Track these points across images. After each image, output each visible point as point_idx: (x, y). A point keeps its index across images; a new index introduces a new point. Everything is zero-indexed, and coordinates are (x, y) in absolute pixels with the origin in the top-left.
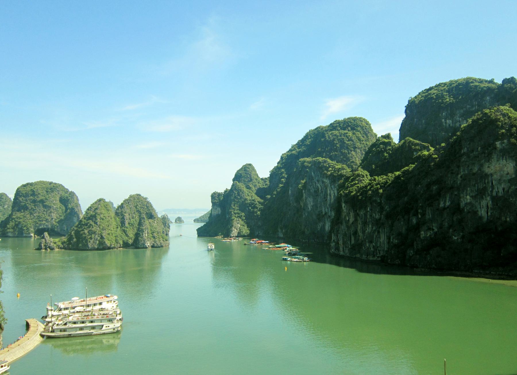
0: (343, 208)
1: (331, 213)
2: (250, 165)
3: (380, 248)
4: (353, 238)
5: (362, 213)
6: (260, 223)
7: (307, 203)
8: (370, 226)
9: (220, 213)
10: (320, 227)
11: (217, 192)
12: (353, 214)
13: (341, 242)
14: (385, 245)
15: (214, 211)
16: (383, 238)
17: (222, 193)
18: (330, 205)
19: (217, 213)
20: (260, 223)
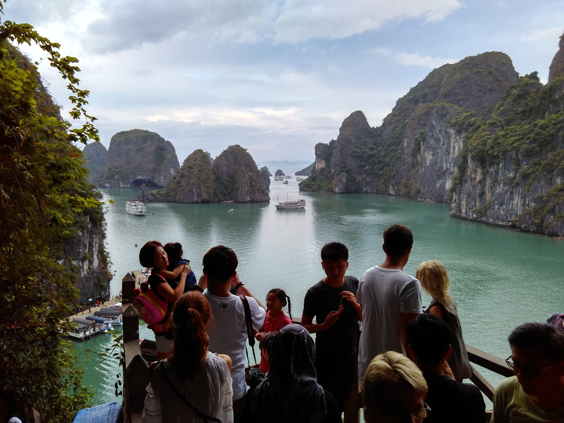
0: (469, 164)
1: (453, 169)
3: (512, 211)
4: (478, 199)
5: (492, 170)
7: (425, 156)
8: (502, 185)
9: (324, 166)
13: (464, 202)
14: (519, 208)
15: (318, 165)
16: (517, 200)
17: (327, 144)
18: (452, 159)
19: (322, 167)
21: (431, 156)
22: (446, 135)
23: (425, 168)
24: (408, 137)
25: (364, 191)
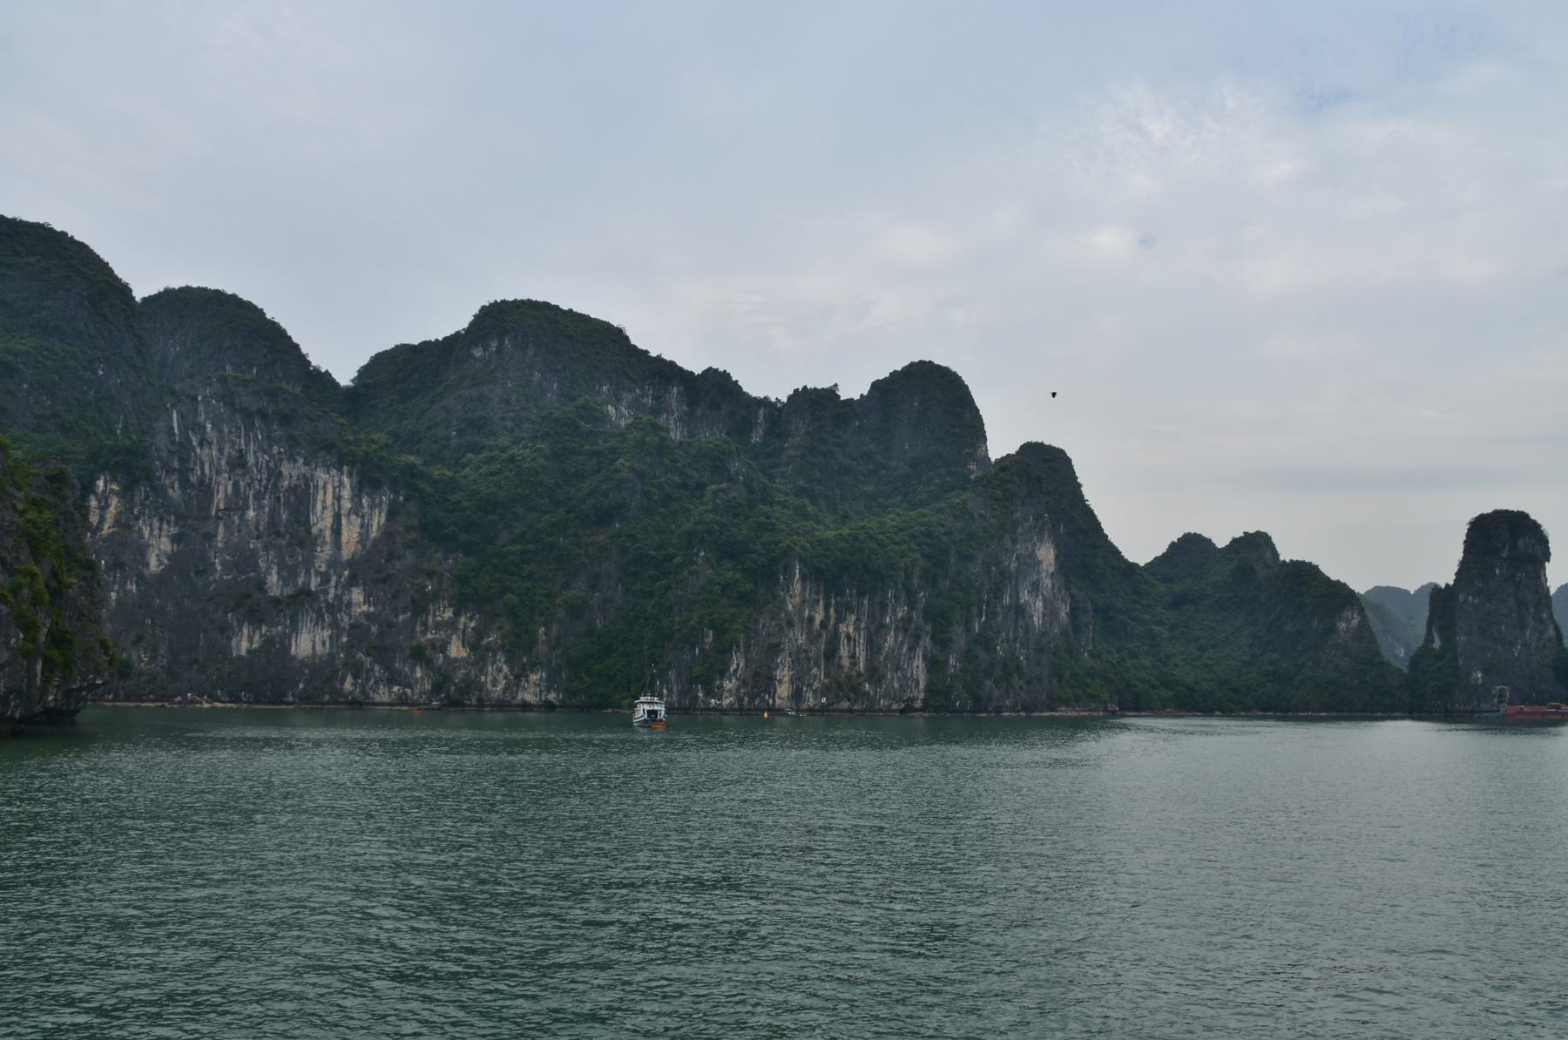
23: (141, 580)
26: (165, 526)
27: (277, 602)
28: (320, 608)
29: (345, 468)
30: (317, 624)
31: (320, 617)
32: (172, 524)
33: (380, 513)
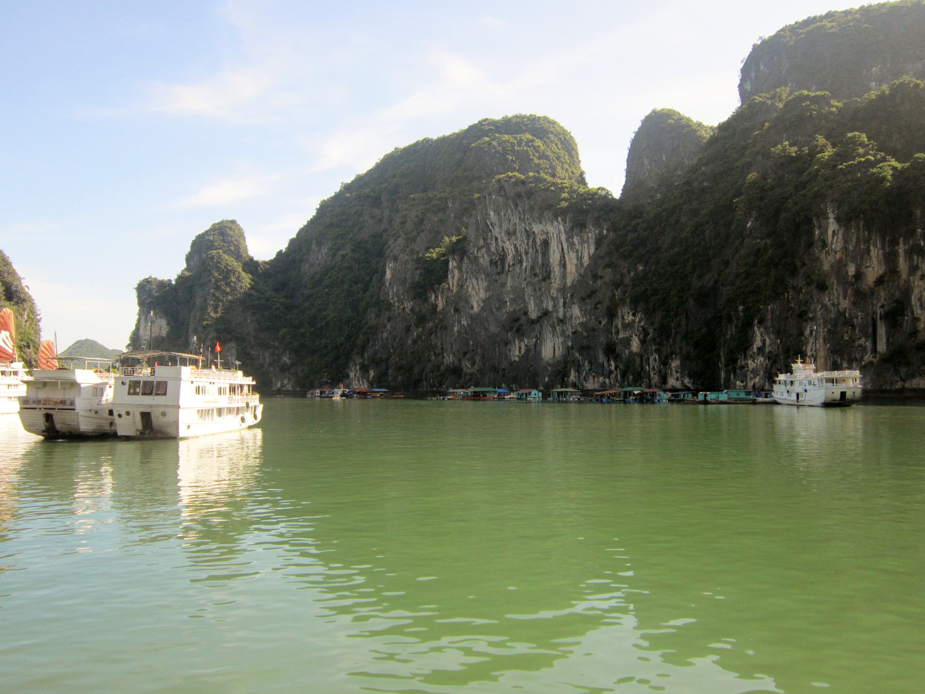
2: (233, 222)
4: (882, 331)
6: (286, 359)
9: (164, 333)
10: (520, 352)
11: (155, 279)
12: (881, 252)
17: (170, 281)
19: (157, 335)
20: (286, 359)
21: (482, 291)
22: (528, 240)
24: (395, 259)
25: (275, 389)
26: (480, 282)
27: (533, 322)
28: (554, 323)
29: (559, 219)
30: (554, 335)
31: (553, 327)
32: (484, 280)
33: (589, 246)
